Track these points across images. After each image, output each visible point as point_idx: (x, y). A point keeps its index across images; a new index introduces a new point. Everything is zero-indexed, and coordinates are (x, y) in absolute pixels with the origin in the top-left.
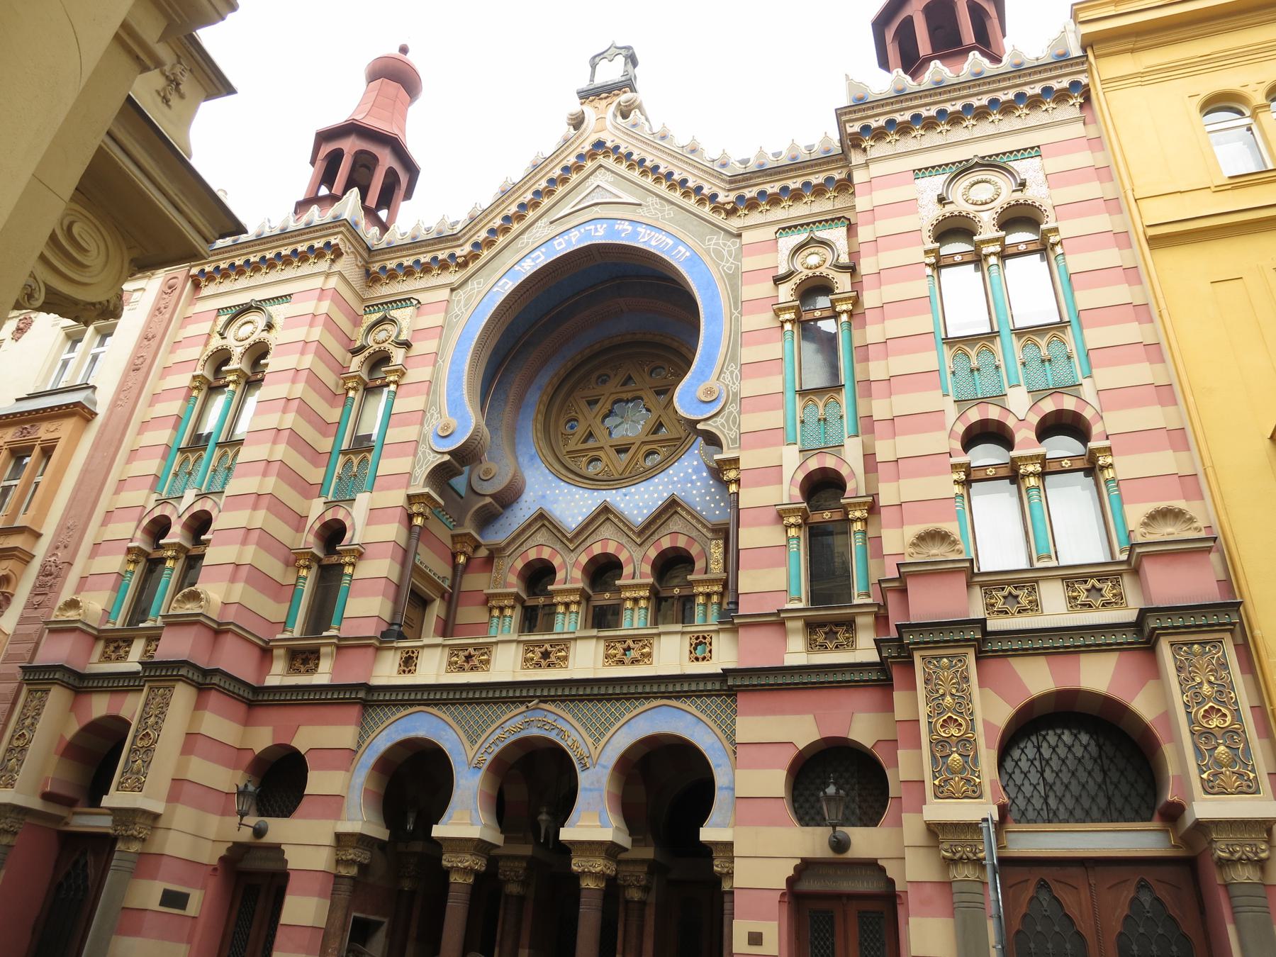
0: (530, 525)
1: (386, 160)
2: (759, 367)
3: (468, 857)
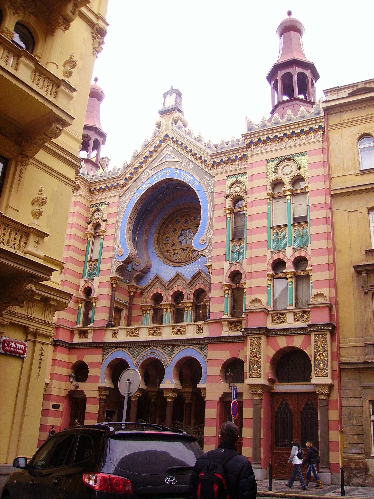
0: (153, 281)
1: (93, 136)
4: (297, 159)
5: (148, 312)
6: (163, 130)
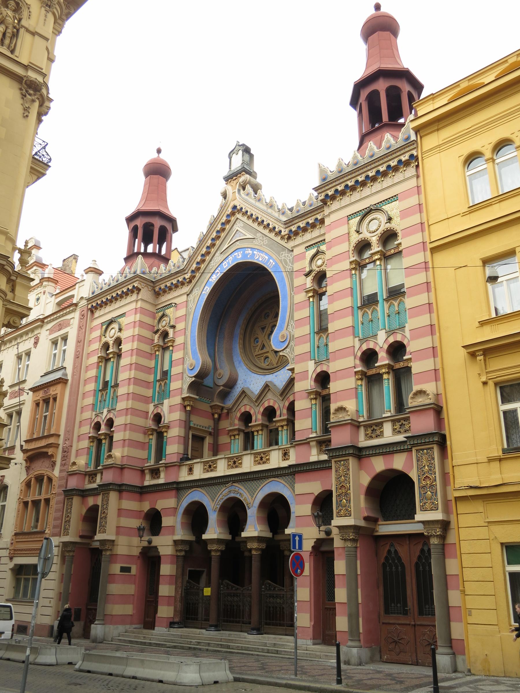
0: (240, 396)
1: (158, 223)
2: (300, 322)
3: (215, 545)
4: (385, 208)
5: (237, 437)
6: (230, 200)
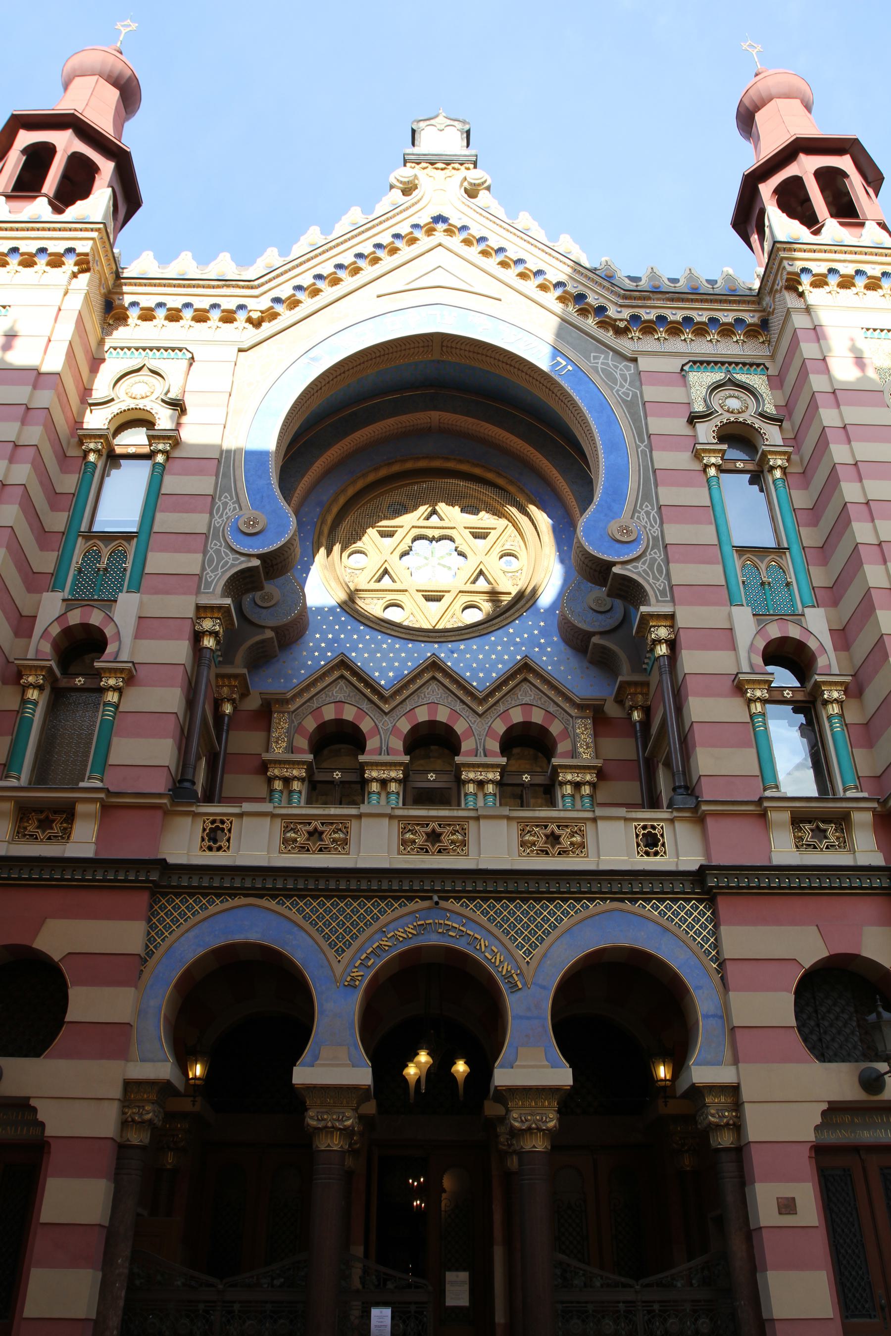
5: (296, 785)
